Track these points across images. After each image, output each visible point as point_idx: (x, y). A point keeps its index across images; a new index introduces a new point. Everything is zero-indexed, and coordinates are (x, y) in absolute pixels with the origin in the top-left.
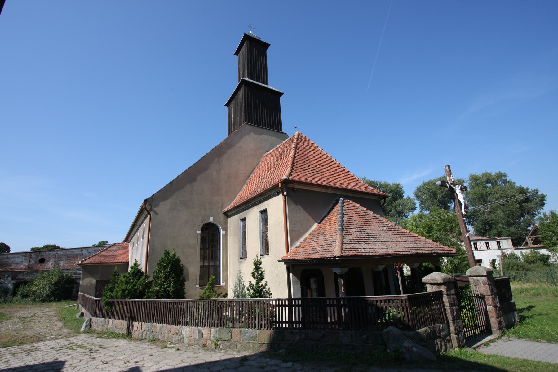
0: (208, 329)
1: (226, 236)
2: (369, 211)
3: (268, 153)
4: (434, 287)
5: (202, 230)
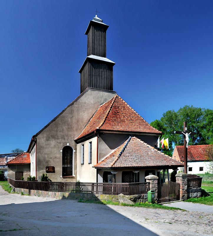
0: (58, 193)
1: (76, 152)
2: (145, 143)
3: (102, 105)
4: (149, 180)
5: (63, 150)
